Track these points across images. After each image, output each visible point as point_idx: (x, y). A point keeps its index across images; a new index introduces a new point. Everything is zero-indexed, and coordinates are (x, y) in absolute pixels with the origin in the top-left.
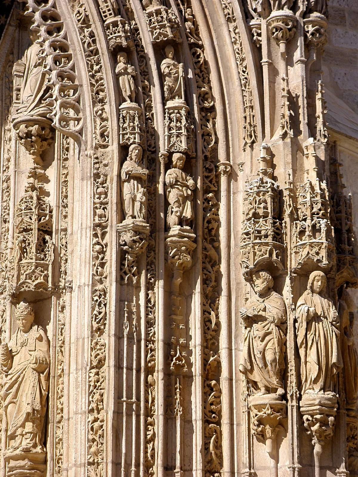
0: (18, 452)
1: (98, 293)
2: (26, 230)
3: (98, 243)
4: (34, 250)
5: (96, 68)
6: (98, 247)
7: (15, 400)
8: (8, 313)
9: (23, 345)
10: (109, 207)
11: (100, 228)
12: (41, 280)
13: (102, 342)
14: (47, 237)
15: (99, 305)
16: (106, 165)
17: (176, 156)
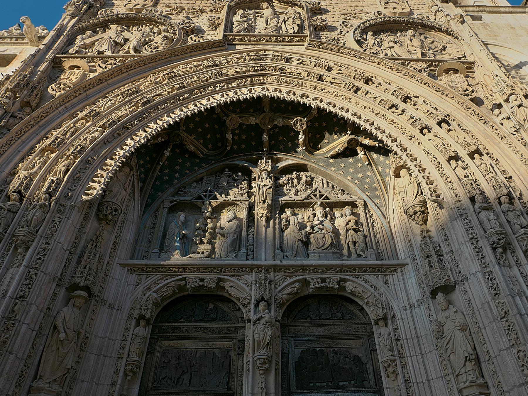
0: (467, 384)
1: (487, 274)
2: (428, 257)
3: (476, 247)
4: (437, 264)
5: (441, 170)
6: (477, 250)
7: (453, 351)
8: (431, 305)
9: (447, 318)
10: (475, 228)
11: (474, 240)
12: (446, 278)
13: (502, 301)
14: (442, 257)
15: (491, 280)
16: (464, 209)
17: (502, 199)
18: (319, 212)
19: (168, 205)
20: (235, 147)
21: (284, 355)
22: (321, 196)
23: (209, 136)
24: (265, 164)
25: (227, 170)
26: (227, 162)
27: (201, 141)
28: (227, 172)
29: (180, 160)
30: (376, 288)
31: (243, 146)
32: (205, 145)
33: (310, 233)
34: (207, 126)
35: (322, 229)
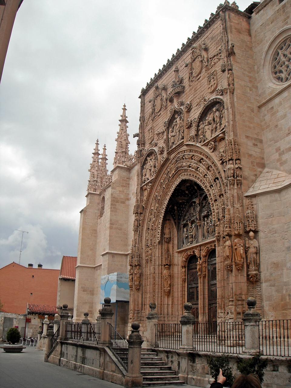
19: (182, 226)
21: (208, 270)
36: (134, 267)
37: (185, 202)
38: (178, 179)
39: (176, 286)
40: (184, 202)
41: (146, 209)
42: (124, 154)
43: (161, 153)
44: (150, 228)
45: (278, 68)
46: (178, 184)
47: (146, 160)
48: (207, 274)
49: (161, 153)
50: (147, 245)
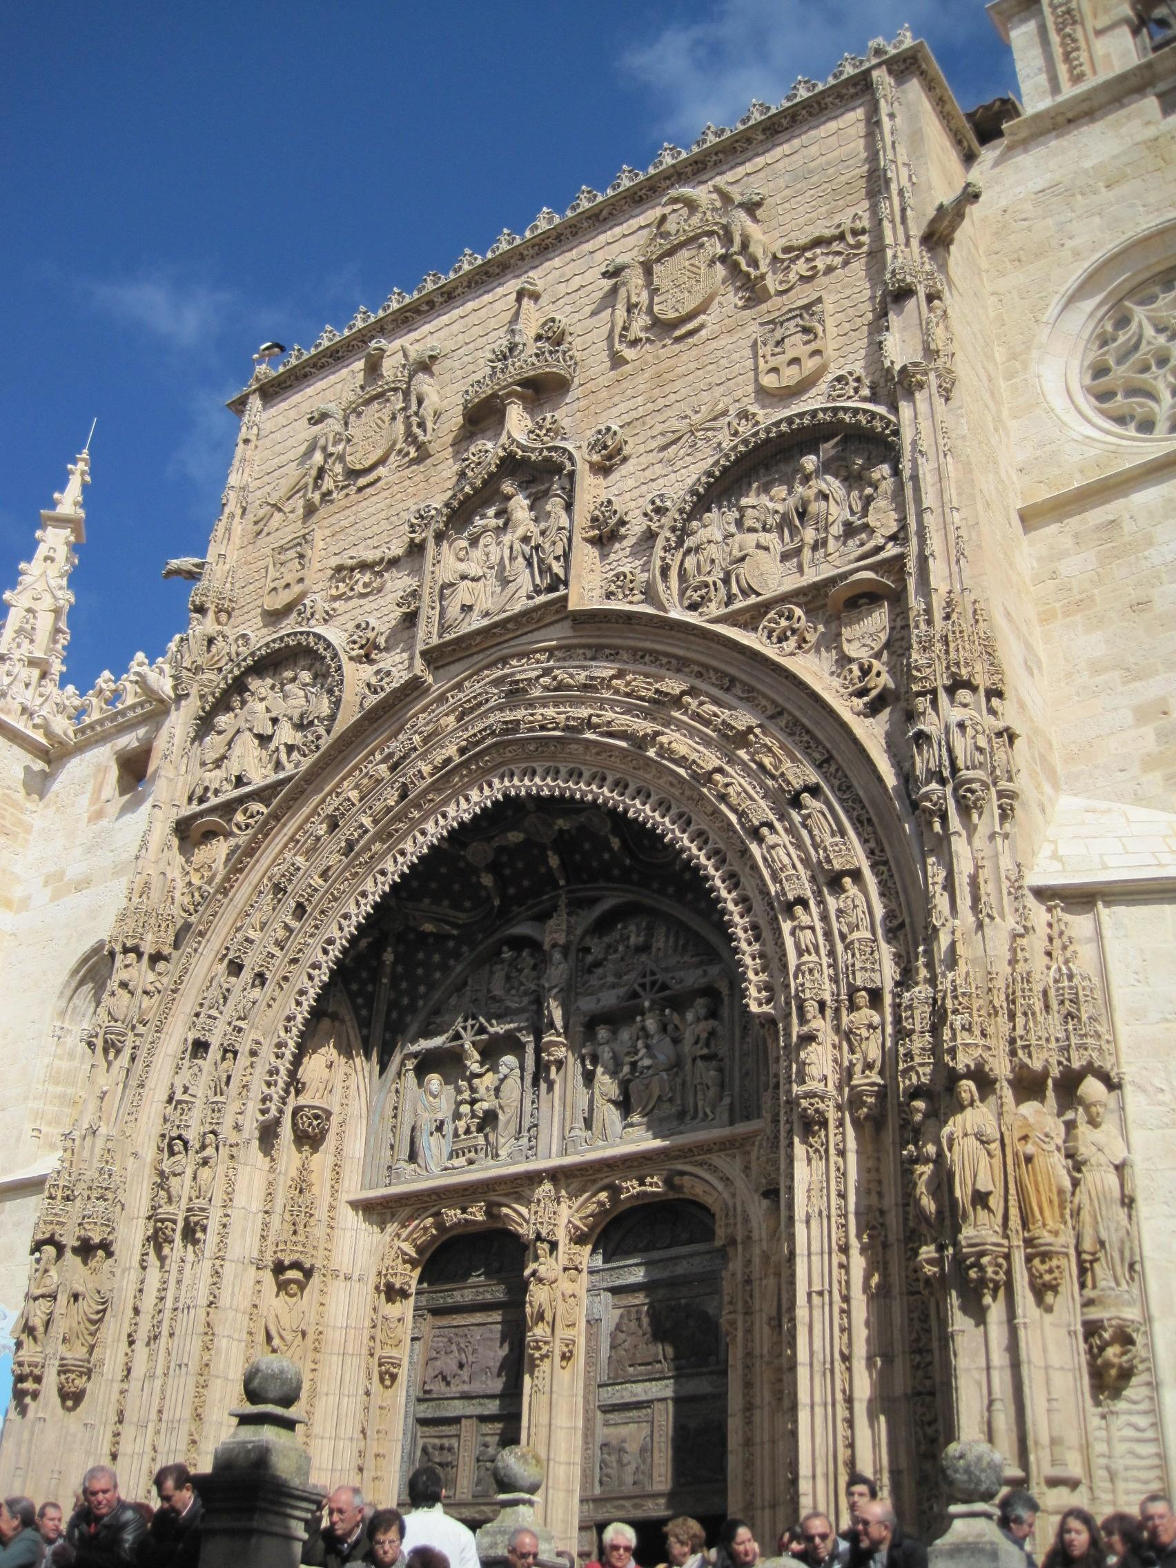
18: (651, 1024)
20: (511, 891)
21: (592, 1323)
22: (653, 983)
23: (456, 887)
24: (554, 932)
25: (505, 949)
26: (498, 935)
27: (446, 903)
28: (507, 954)
29: (421, 956)
30: (726, 1180)
31: (526, 883)
32: (457, 906)
33: (629, 1081)
34: (443, 870)
35: (648, 1068)
36: (68, 1254)
37: (451, 937)
38: (496, 781)
39: (331, 1398)
40: (445, 937)
41: (201, 934)
42: (36, 673)
43: (367, 656)
44: (215, 1041)
45: (1121, 373)
46: (467, 817)
47: (238, 687)
48: (582, 1341)
49: (367, 656)
50: (180, 1137)
